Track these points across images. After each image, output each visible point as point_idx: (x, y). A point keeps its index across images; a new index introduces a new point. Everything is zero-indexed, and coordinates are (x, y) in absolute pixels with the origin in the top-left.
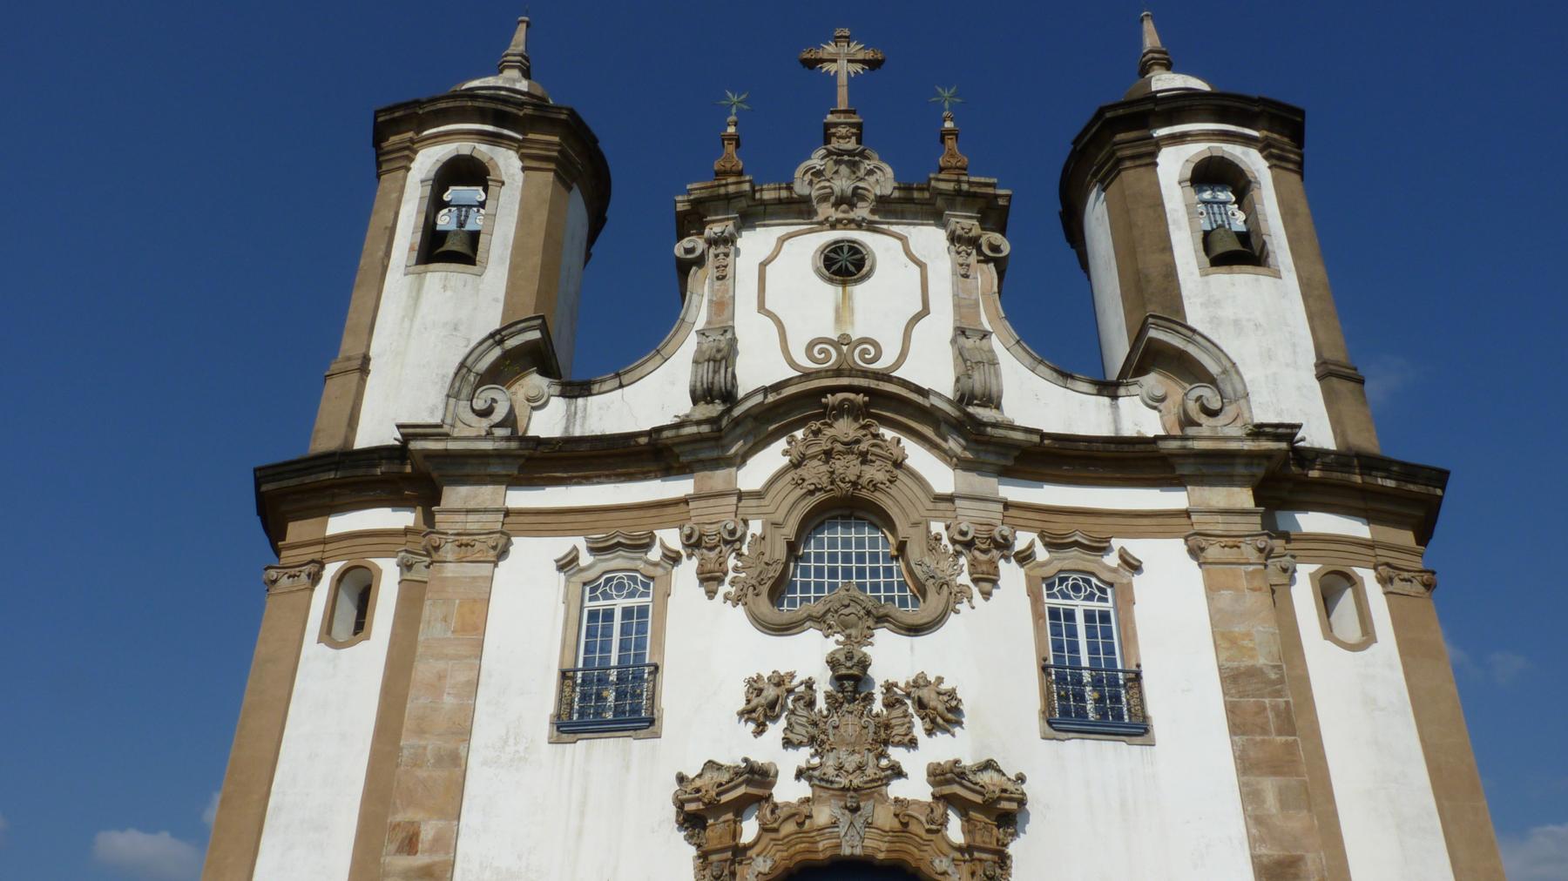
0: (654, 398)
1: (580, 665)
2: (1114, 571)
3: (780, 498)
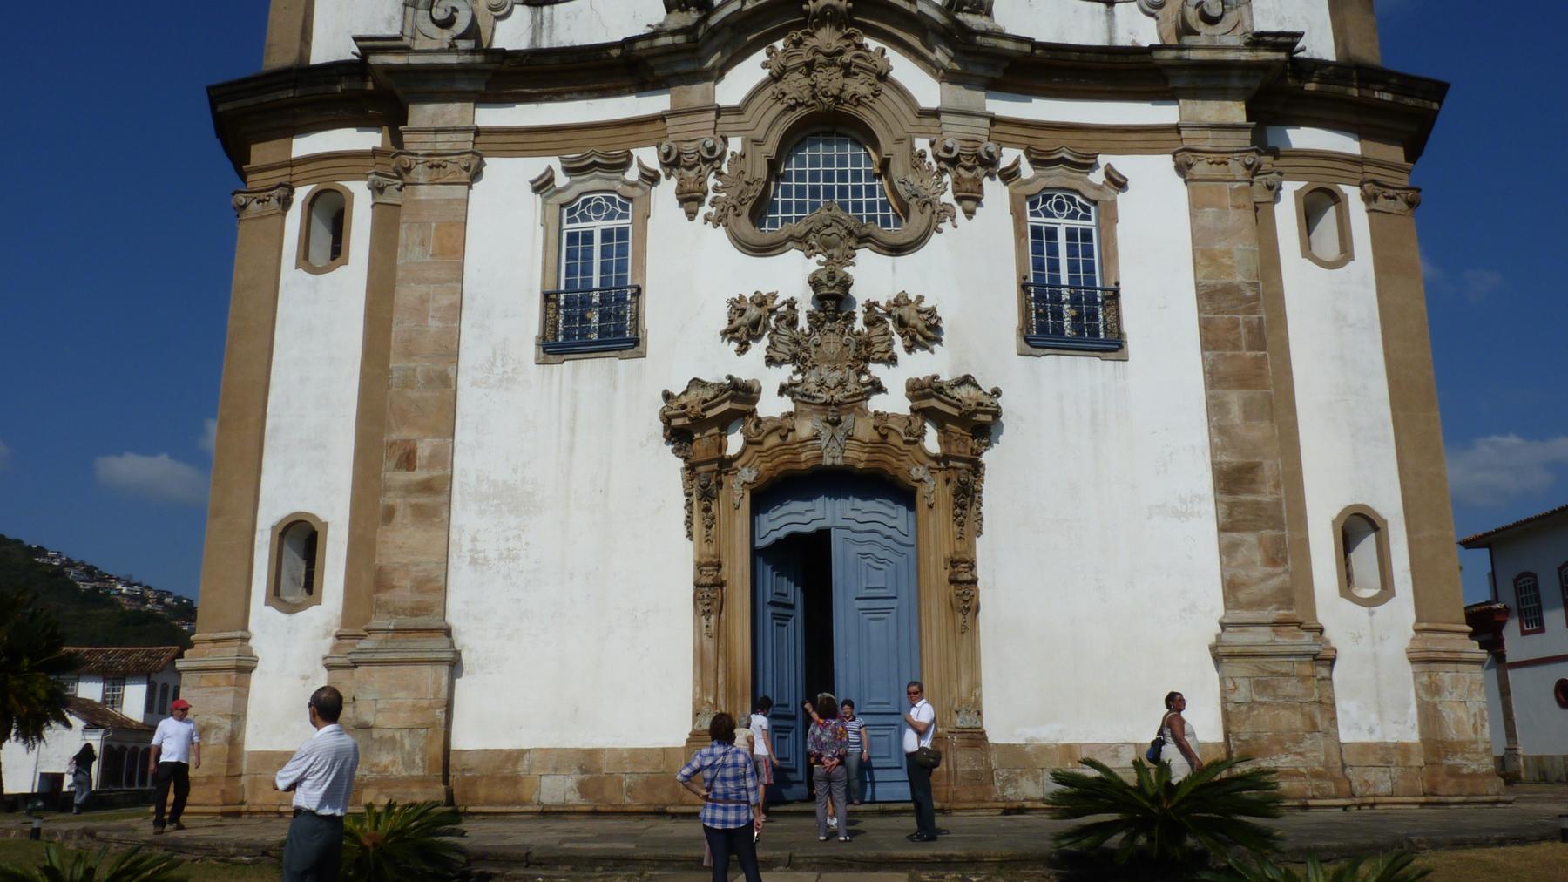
1: (563, 288)
2: (1099, 188)
3: (759, 113)
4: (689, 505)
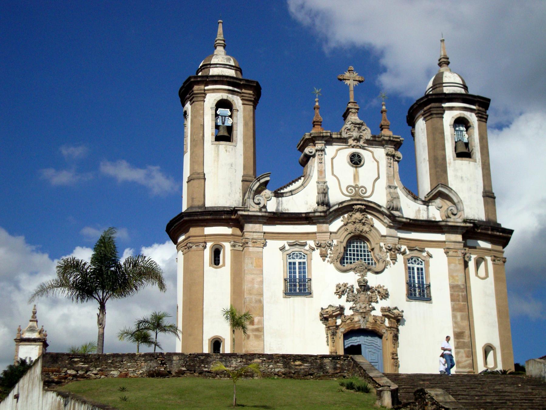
0: (302, 199)
2: (425, 257)
4: (327, 337)
